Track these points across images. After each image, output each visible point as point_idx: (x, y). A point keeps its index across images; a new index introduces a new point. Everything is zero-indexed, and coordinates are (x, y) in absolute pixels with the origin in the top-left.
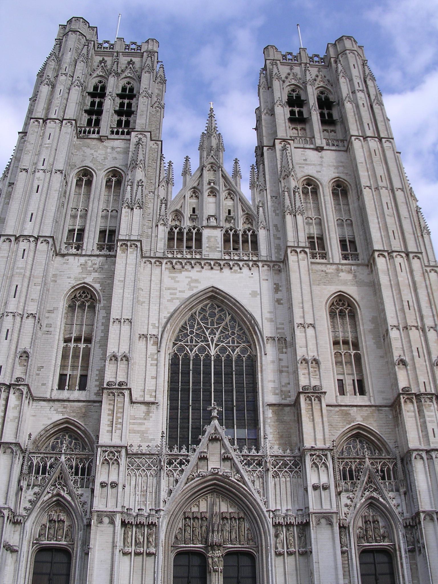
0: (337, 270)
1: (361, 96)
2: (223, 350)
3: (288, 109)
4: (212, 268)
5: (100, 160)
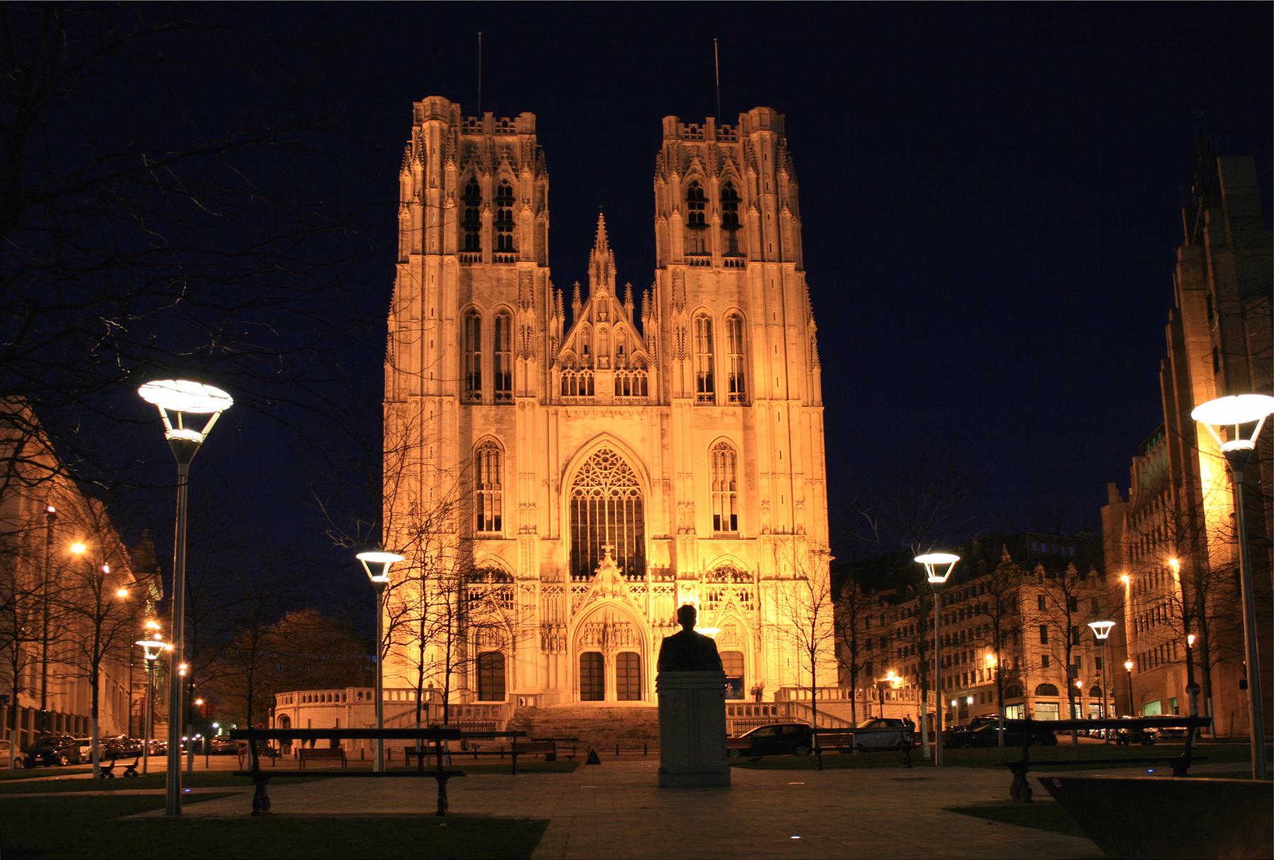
0: (723, 414)
1: (769, 199)
2: (615, 493)
3: (687, 211)
4: (604, 416)
5: (486, 296)
